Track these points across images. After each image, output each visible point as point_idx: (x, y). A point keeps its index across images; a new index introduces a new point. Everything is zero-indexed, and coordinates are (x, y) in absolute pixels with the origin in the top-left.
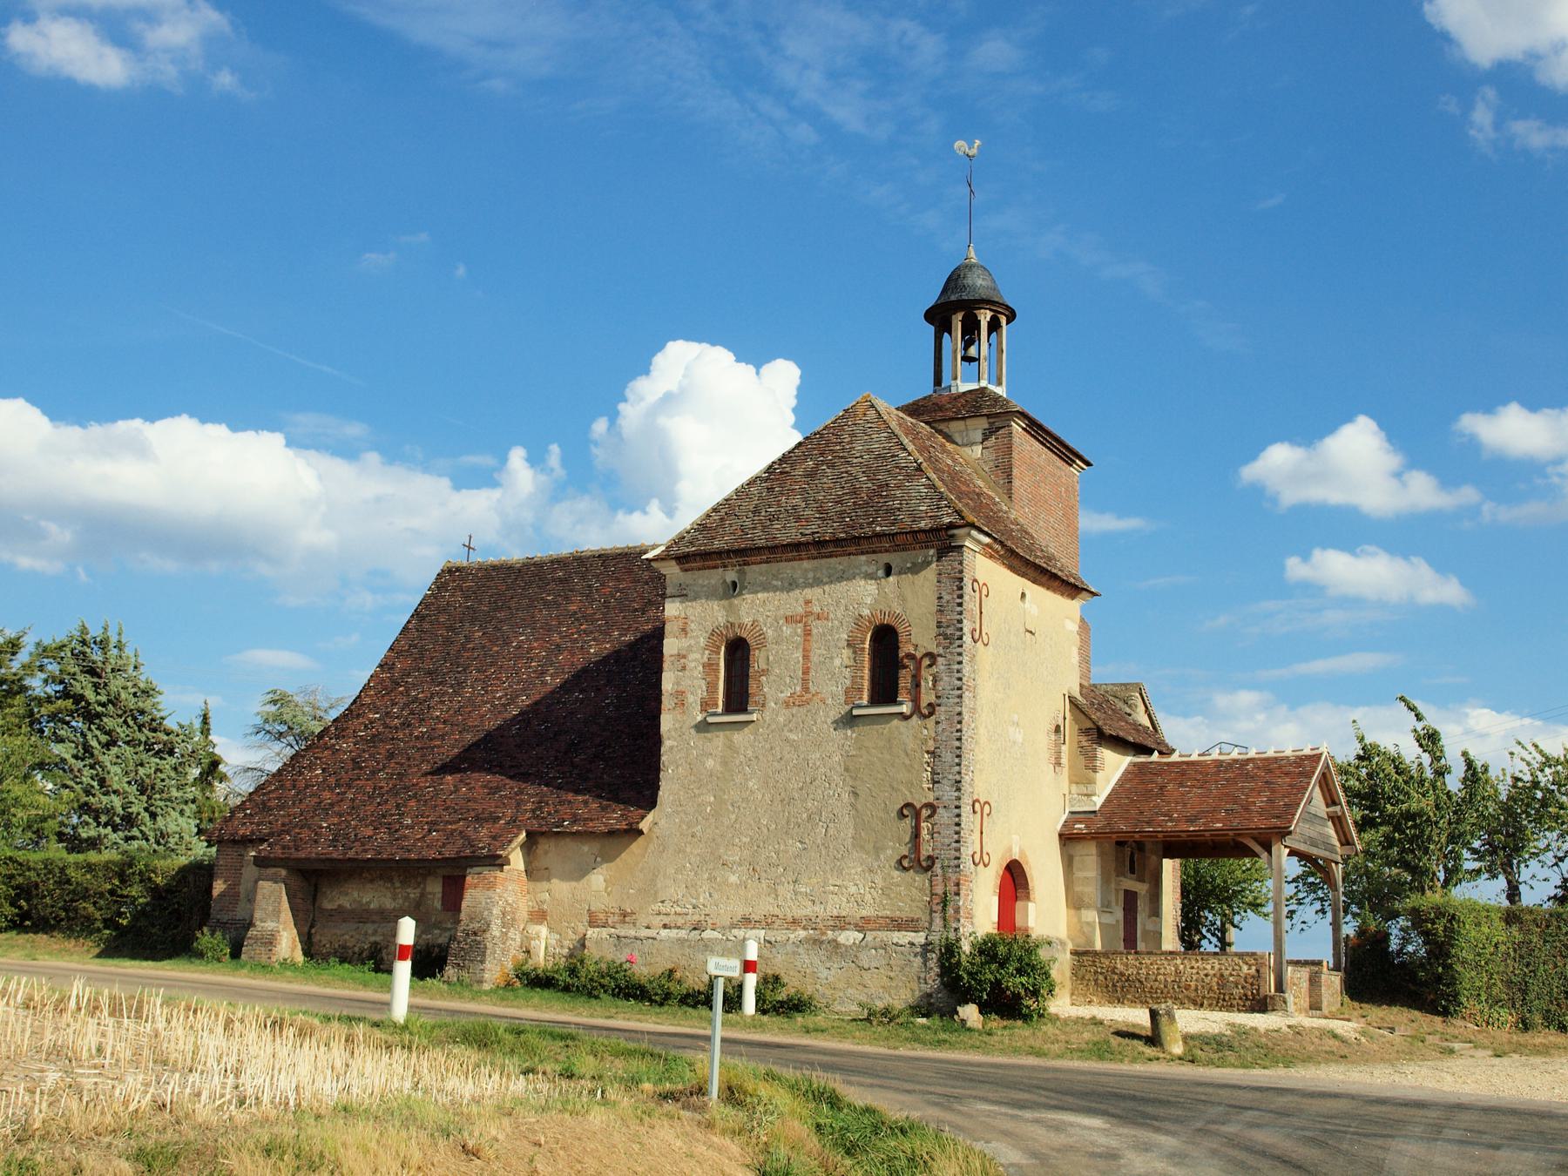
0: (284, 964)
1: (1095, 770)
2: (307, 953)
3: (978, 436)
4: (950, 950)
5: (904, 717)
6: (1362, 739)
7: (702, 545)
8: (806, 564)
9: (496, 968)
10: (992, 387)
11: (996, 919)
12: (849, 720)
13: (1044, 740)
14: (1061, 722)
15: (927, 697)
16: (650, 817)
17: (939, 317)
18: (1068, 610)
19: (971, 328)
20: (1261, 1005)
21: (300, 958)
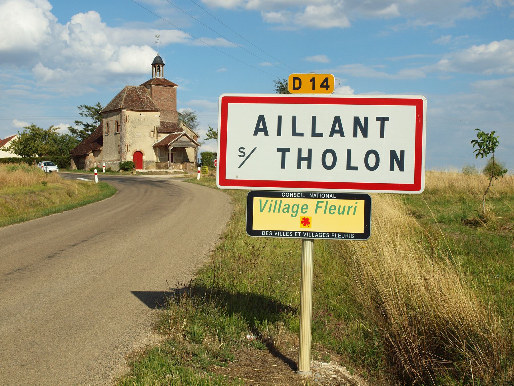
0: (74, 170)
1: (158, 137)
2: (78, 169)
3: (149, 87)
4: (121, 163)
5: (118, 134)
6: (210, 128)
7: (105, 111)
8: (112, 113)
9: (87, 169)
10: (159, 78)
11: (133, 159)
12: (115, 134)
13: (147, 134)
14: (153, 130)
15: (120, 131)
16: (102, 148)
17: (154, 65)
18: (158, 113)
19: (159, 66)
20: (168, 168)
21: (77, 169)
